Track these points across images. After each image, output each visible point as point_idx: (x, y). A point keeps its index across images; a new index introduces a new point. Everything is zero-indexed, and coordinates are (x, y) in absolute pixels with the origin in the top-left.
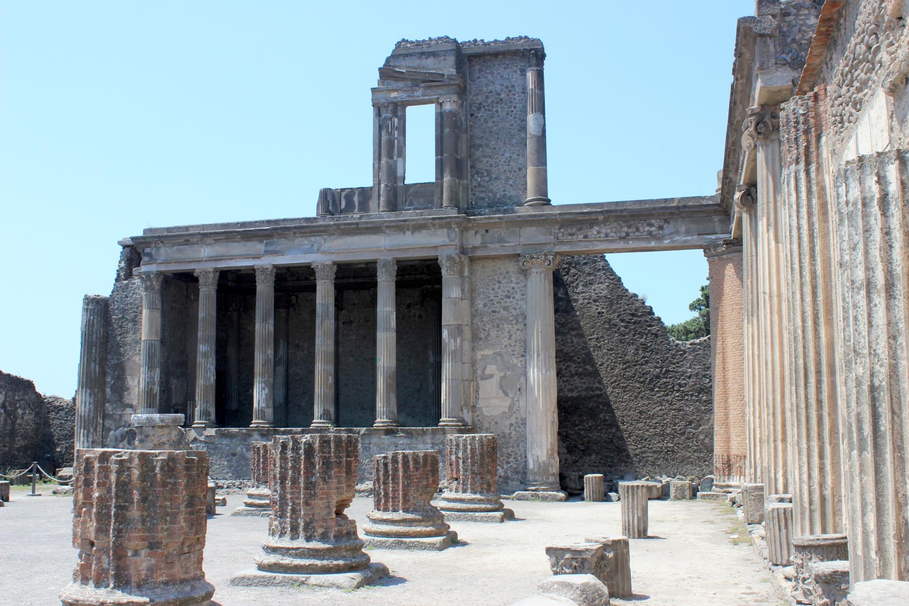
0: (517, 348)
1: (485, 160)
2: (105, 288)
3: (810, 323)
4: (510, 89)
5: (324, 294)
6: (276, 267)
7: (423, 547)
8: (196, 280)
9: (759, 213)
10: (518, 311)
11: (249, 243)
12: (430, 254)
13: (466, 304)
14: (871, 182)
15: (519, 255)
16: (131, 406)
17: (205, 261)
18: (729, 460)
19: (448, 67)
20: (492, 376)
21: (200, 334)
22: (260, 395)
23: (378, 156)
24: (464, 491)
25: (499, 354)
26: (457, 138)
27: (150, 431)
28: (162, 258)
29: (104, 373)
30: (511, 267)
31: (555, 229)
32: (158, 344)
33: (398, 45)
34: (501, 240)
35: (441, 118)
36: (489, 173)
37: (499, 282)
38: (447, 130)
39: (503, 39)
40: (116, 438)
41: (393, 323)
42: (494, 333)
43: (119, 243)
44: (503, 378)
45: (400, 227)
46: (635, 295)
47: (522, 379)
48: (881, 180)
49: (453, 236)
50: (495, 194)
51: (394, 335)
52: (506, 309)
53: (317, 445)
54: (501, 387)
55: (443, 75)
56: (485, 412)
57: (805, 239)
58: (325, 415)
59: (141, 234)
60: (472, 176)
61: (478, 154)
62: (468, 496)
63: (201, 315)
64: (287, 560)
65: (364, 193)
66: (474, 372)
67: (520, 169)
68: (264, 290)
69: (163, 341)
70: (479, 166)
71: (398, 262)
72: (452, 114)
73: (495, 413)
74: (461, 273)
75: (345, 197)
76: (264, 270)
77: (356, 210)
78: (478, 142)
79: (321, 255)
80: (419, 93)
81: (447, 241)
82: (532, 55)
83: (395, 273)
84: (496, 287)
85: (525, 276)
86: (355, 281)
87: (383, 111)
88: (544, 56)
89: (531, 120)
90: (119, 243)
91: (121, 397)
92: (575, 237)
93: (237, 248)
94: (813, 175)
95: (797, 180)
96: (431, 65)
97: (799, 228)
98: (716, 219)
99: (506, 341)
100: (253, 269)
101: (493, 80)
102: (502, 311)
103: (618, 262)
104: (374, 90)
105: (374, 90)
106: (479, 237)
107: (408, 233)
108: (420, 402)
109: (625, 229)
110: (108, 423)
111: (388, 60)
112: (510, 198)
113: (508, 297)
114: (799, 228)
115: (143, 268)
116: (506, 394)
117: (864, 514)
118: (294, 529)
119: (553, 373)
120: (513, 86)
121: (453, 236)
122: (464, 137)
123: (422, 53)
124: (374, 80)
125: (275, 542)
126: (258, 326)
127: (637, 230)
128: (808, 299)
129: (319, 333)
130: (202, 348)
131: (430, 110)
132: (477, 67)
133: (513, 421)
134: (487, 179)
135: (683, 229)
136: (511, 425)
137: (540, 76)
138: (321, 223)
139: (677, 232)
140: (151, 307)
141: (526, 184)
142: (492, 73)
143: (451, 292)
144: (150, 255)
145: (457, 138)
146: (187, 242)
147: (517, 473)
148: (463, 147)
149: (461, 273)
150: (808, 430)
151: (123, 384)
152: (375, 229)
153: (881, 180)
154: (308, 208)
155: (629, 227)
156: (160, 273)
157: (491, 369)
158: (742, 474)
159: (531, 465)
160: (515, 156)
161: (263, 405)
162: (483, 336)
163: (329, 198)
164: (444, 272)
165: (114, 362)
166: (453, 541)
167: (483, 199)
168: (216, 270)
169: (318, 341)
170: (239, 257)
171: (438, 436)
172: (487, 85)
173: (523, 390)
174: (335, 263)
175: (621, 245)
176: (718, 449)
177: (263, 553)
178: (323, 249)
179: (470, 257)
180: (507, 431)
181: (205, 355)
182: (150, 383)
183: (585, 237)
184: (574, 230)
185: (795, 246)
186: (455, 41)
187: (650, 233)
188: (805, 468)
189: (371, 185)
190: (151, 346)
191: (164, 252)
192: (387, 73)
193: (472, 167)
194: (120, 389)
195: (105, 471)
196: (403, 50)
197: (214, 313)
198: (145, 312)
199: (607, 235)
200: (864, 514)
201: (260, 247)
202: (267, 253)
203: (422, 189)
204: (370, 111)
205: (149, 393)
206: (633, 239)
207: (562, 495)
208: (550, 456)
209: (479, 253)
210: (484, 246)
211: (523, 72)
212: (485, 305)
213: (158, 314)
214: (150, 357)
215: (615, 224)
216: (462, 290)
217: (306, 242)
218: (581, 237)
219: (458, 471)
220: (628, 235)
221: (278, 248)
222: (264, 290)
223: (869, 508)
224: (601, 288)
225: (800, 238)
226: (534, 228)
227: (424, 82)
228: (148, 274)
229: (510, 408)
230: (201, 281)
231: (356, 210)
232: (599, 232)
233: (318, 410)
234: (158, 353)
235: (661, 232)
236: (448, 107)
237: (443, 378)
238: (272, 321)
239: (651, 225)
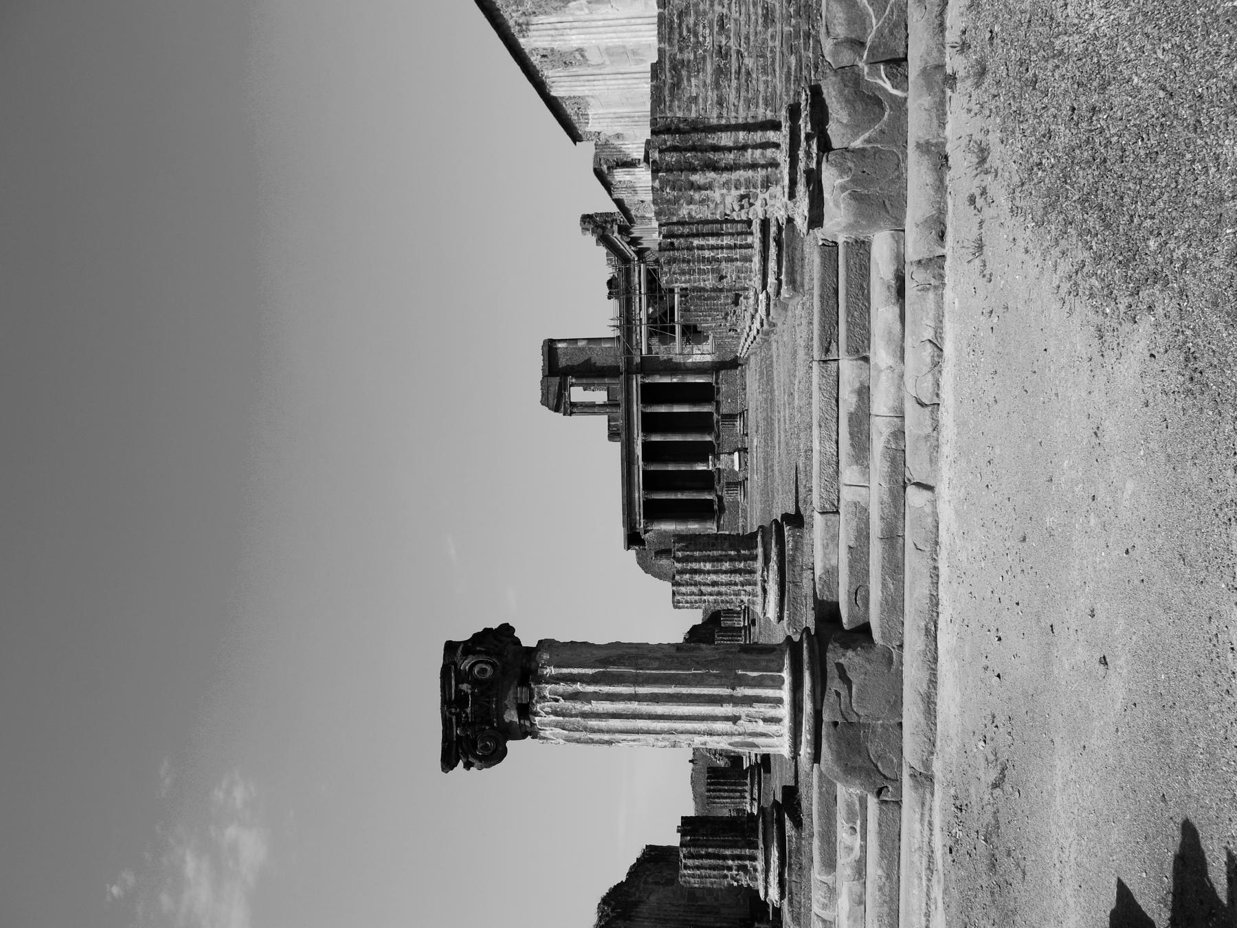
4: (565, 354)
5: (656, 438)
17: (639, 495)
19: (557, 380)
23: (594, 413)
58: (709, 434)
82: (550, 348)
86: (651, 423)
89: (581, 344)
96: (554, 389)
108: (706, 394)
126: (671, 468)
130: (680, 496)
137: (560, 341)
192: (557, 410)
196: (545, 402)
204: (574, 417)
233: (708, 438)
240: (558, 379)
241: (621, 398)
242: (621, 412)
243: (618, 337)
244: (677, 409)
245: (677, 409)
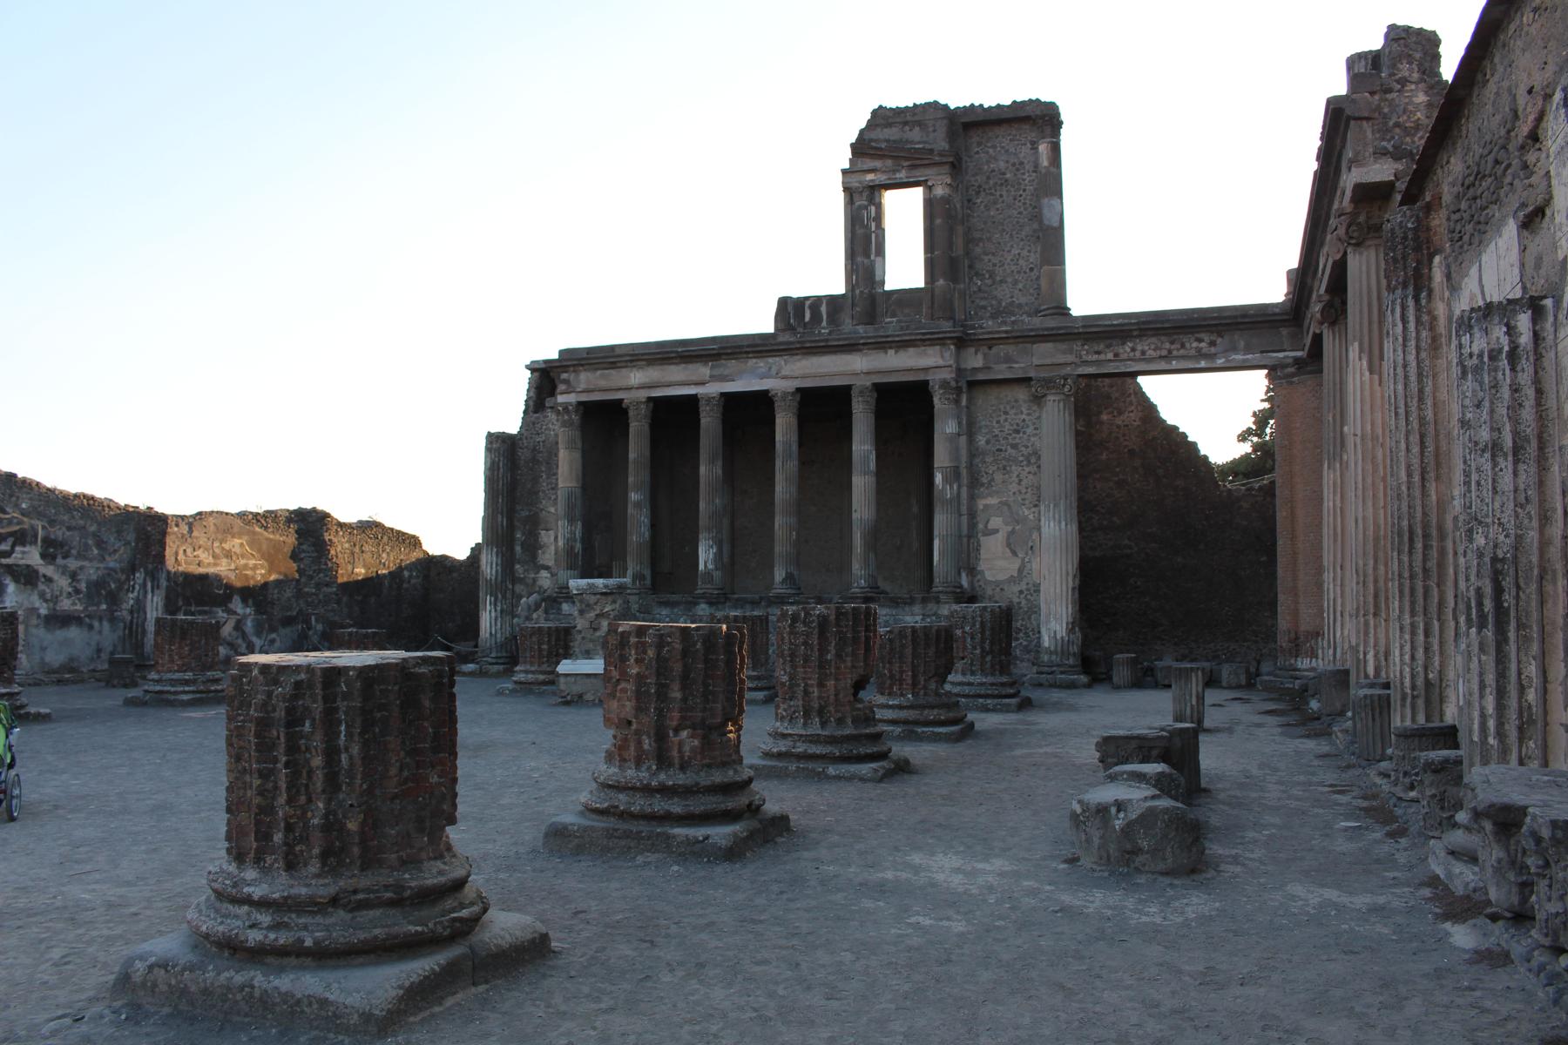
0: (1028, 496)
1: (986, 258)
2: (513, 426)
3: (1417, 478)
5: (784, 426)
6: (722, 394)
7: (936, 738)
8: (625, 412)
9: (1350, 336)
10: (1030, 450)
11: (690, 366)
12: (921, 377)
13: (963, 439)
14: (1499, 332)
15: (1030, 379)
16: (547, 568)
17: (635, 384)
18: (1297, 638)
19: (940, 142)
20: (997, 531)
21: (631, 479)
22: (706, 556)
24: (973, 673)
25: (1006, 504)
26: (951, 230)
27: (593, 599)
28: (582, 386)
29: (511, 527)
30: (1021, 394)
31: (1077, 346)
32: (578, 491)
33: (874, 113)
34: (1008, 359)
35: (930, 205)
36: (992, 275)
37: (1006, 413)
38: (938, 221)
39: (1008, 102)
40: (529, 607)
41: (873, 466)
42: (999, 477)
43: (527, 367)
44: (1013, 532)
45: (882, 345)
46: (1176, 428)
47: (1035, 535)
48: (1511, 331)
49: (947, 355)
50: (1000, 303)
51: (874, 479)
52: (1014, 446)
53: (833, 617)
54: (1009, 545)
55: (932, 151)
56: (989, 576)
57: (1413, 378)
58: (789, 578)
59: (556, 356)
60: (971, 279)
61: (978, 250)
62: (978, 679)
63: (632, 456)
64: (801, 748)
65: (832, 300)
66: (972, 526)
67: (1031, 269)
68: (709, 421)
69: (584, 488)
70: (978, 266)
71: (877, 387)
72: (946, 200)
73: (1001, 577)
74: (957, 401)
75: (810, 307)
76: (709, 399)
77: (824, 323)
78: (977, 235)
79: (779, 378)
80: (902, 175)
81: (941, 363)
83: (873, 402)
84: (1002, 419)
85: (1039, 405)
87: (856, 197)
88: (1060, 123)
90: (527, 367)
91: (534, 557)
92: (1102, 357)
93: (676, 372)
94: (1423, 302)
95: (1404, 308)
97: (1405, 366)
98: (1285, 332)
99: (1014, 487)
100: (695, 396)
101: (997, 153)
102: (1010, 450)
103: (1155, 387)
104: (844, 172)
105: (844, 172)
106: (980, 356)
107: (891, 352)
109: (1167, 345)
110: (519, 588)
111: (862, 132)
112: (1020, 306)
113: (1017, 432)
114: (1405, 366)
115: (561, 399)
116: (1014, 553)
117: (1482, 696)
118: (807, 715)
119: (1074, 528)
120: (1022, 163)
121: (947, 355)
122: (960, 229)
123: (906, 123)
124: (844, 159)
125: (783, 728)
126: (703, 469)
127: (1183, 346)
128: (1416, 450)
129: (779, 477)
130: (634, 496)
131: (918, 193)
132: (975, 139)
133: (1024, 587)
134: (989, 282)
135: (1242, 343)
136: (1021, 592)
138: (781, 339)
139: (1234, 349)
140: (570, 446)
141: (1039, 288)
142: (994, 147)
143: (946, 427)
144: (567, 382)
145: (951, 230)
146: (613, 365)
147: (1029, 652)
148: (959, 241)
149: (957, 401)
150: (1413, 603)
151: (536, 540)
152: (850, 347)
153: (1511, 331)
154: (765, 324)
155: (1172, 343)
156: (580, 403)
157: (996, 522)
158: (1313, 655)
159: (1046, 642)
160: (1025, 253)
161: (710, 567)
162: (984, 480)
163: (790, 308)
164: (936, 400)
165: (525, 513)
166: (968, 731)
167: (984, 307)
168: (650, 399)
169: (778, 488)
170: (678, 382)
171: (930, 606)
172: (988, 162)
173: (1036, 549)
174: (798, 390)
175: (1163, 365)
176: (1283, 623)
177: (770, 740)
178: (784, 373)
179: (974, 385)
180: (1016, 600)
181: (638, 505)
182: (570, 541)
183: (1116, 355)
184: (1102, 346)
185: (1400, 387)
186: (946, 107)
187: (1199, 350)
188: (1407, 648)
189: (842, 291)
190: (570, 495)
191: (584, 379)
192: (861, 148)
193: (970, 267)
194: (533, 547)
195: (642, 648)
196: (882, 117)
197: (648, 453)
198: (563, 454)
199: (1143, 353)
200: (1482, 696)
201: (704, 371)
202: (713, 378)
203: (906, 297)
204: (840, 198)
205: (570, 551)
206: (1177, 358)
207: (1084, 679)
208: (1071, 631)
209: (981, 377)
210: (987, 368)
211: (1035, 148)
212: (988, 442)
213: (577, 455)
214: (570, 507)
215: (1154, 340)
216: (960, 423)
217: (762, 364)
218: (1110, 356)
219: (965, 648)
220: (1170, 352)
221: (726, 372)
222: (709, 421)
223: (1488, 690)
224: (1132, 417)
225: (1406, 377)
226: (1050, 345)
227: (907, 159)
228: (566, 406)
229: (1020, 571)
230: (631, 413)
231: (824, 323)
232: (1133, 350)
233: (779, 574)
234: (579, 503)
235: (1213, 350)
236: (939, 191)
237: (936, 532)
238: (720, 463)
239: (1200, 340)
240: (943, 145)
241: (891, 325)
242: (850, 327)
243: (1063, 310)
244: (862, 485)
245: (862, 485)
